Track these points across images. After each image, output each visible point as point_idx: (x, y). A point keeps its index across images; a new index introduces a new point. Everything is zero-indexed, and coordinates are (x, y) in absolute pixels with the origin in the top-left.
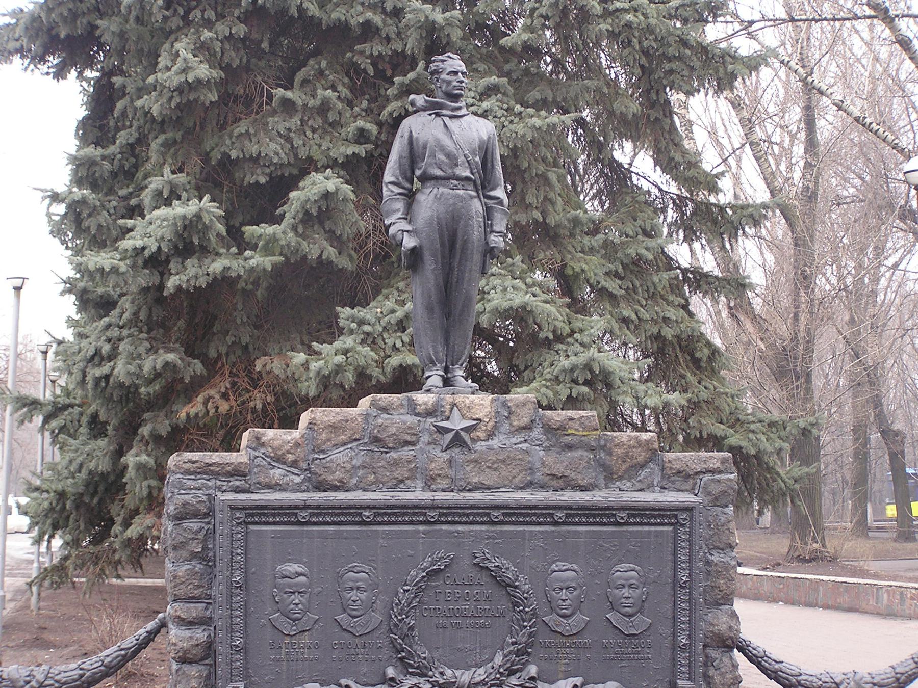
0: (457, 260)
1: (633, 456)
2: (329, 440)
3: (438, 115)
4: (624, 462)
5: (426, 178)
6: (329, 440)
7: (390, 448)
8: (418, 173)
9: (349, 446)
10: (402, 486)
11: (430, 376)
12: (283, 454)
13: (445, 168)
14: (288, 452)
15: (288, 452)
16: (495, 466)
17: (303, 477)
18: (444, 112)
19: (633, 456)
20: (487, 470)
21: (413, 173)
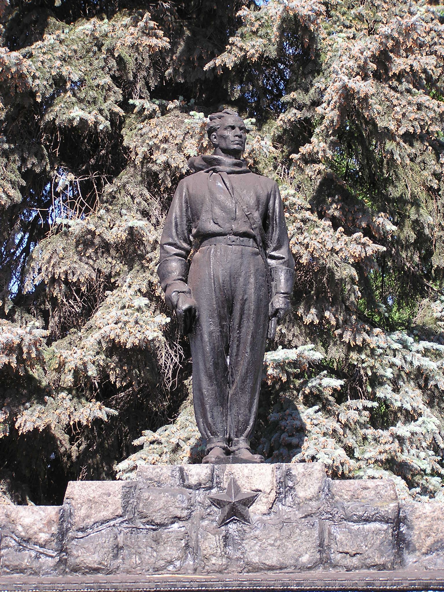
0: (237, 321)
1: (437, 529)
2: (88, 517)
3: (215, 171)
4: (428, 536)
5: (204, 237)
6: (88, 517)
7: (157, 524)
8: (194, 231)
9: (112, 523)
10: (171, 568)
11: (211, 449)
12: (35, 533)
13: (220, 222)
14: (41, 530)
15: (41, 530)
16: (279, 542)
17: (57, 559)
18: (220, 168)
19: (437, 529)
20: (270, 548)
21: (190, 231)
